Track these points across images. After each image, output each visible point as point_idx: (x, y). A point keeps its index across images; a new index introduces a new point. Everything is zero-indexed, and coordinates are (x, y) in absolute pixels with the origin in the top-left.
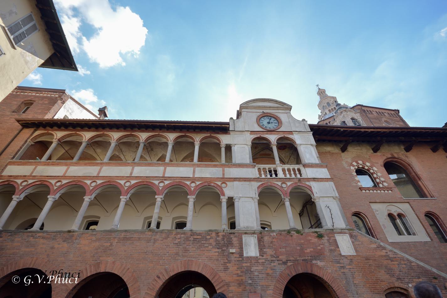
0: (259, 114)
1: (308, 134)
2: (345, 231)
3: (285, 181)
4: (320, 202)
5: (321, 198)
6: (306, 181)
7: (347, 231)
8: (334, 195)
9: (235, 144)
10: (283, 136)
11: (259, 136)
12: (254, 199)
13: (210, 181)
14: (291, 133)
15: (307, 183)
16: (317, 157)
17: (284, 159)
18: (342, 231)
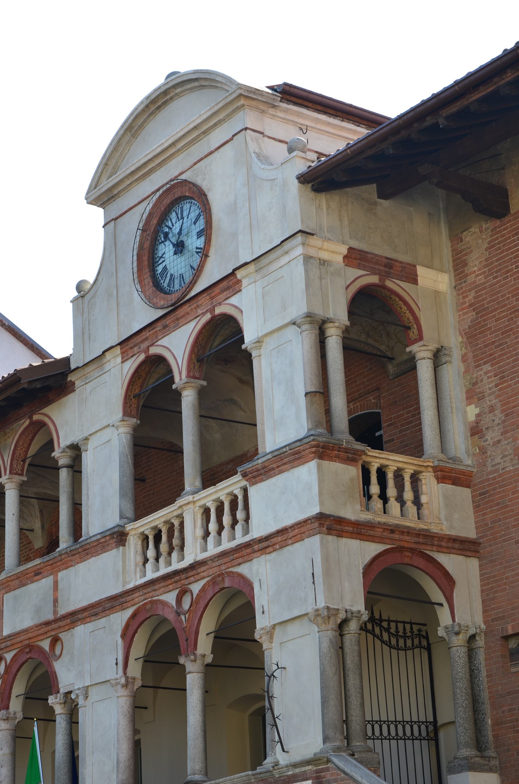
0: (147, 207)
1: (287, 253)
2: (303, 769)
3: (186, 582)
4: (273, 649)
5: (277, 629)
6: (240, 560)
7: (310, 767)
8: (309, 608)
9: (87, 439)
10: (208, 316)
11: (142, 357)
12: (117, 684)
13: (27, 642)
14: (232, 280)
15: (244, 569)
16: (306, 394)
17: (370, 341)
18: (297, 770)
